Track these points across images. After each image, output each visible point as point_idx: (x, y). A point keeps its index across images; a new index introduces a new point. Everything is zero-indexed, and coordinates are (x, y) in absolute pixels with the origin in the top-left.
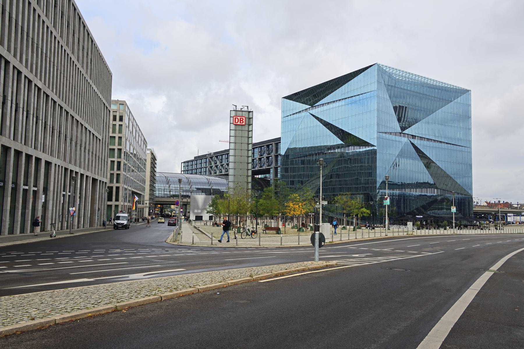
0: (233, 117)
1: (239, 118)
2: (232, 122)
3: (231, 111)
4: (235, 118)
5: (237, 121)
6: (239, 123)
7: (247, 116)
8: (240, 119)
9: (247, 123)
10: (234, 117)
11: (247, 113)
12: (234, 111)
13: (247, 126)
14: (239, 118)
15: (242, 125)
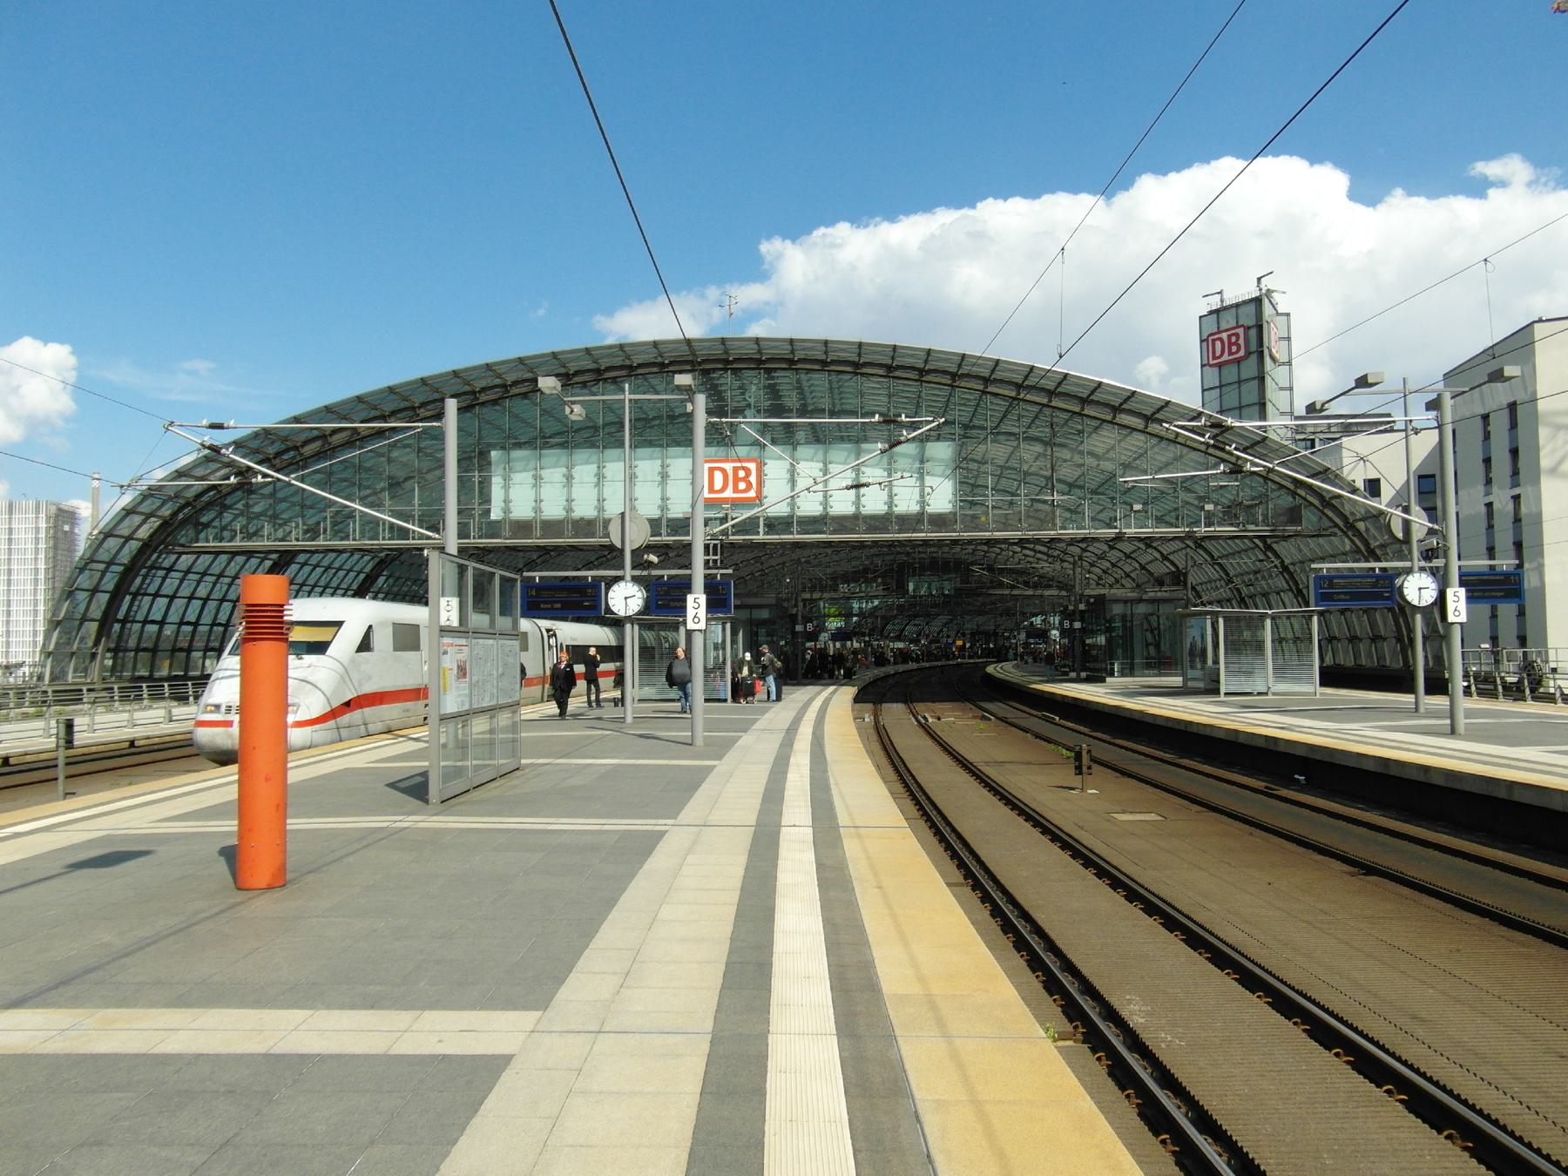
0: (1207, 340)
1: (1224, 336)
2: (1205, 362)
3: (1201, 317)
4: (1214, 341)
5: (1218, 354)
6: (1226, 357)
7: (1251, 322)
8: (1229, 337)
9: (1253, 347)
10: (1210, 338)
11: (1252, 308)
12: (1215, 315)
13: (1254, 358)
14: (1224, 336)
15: (1238, 361)
